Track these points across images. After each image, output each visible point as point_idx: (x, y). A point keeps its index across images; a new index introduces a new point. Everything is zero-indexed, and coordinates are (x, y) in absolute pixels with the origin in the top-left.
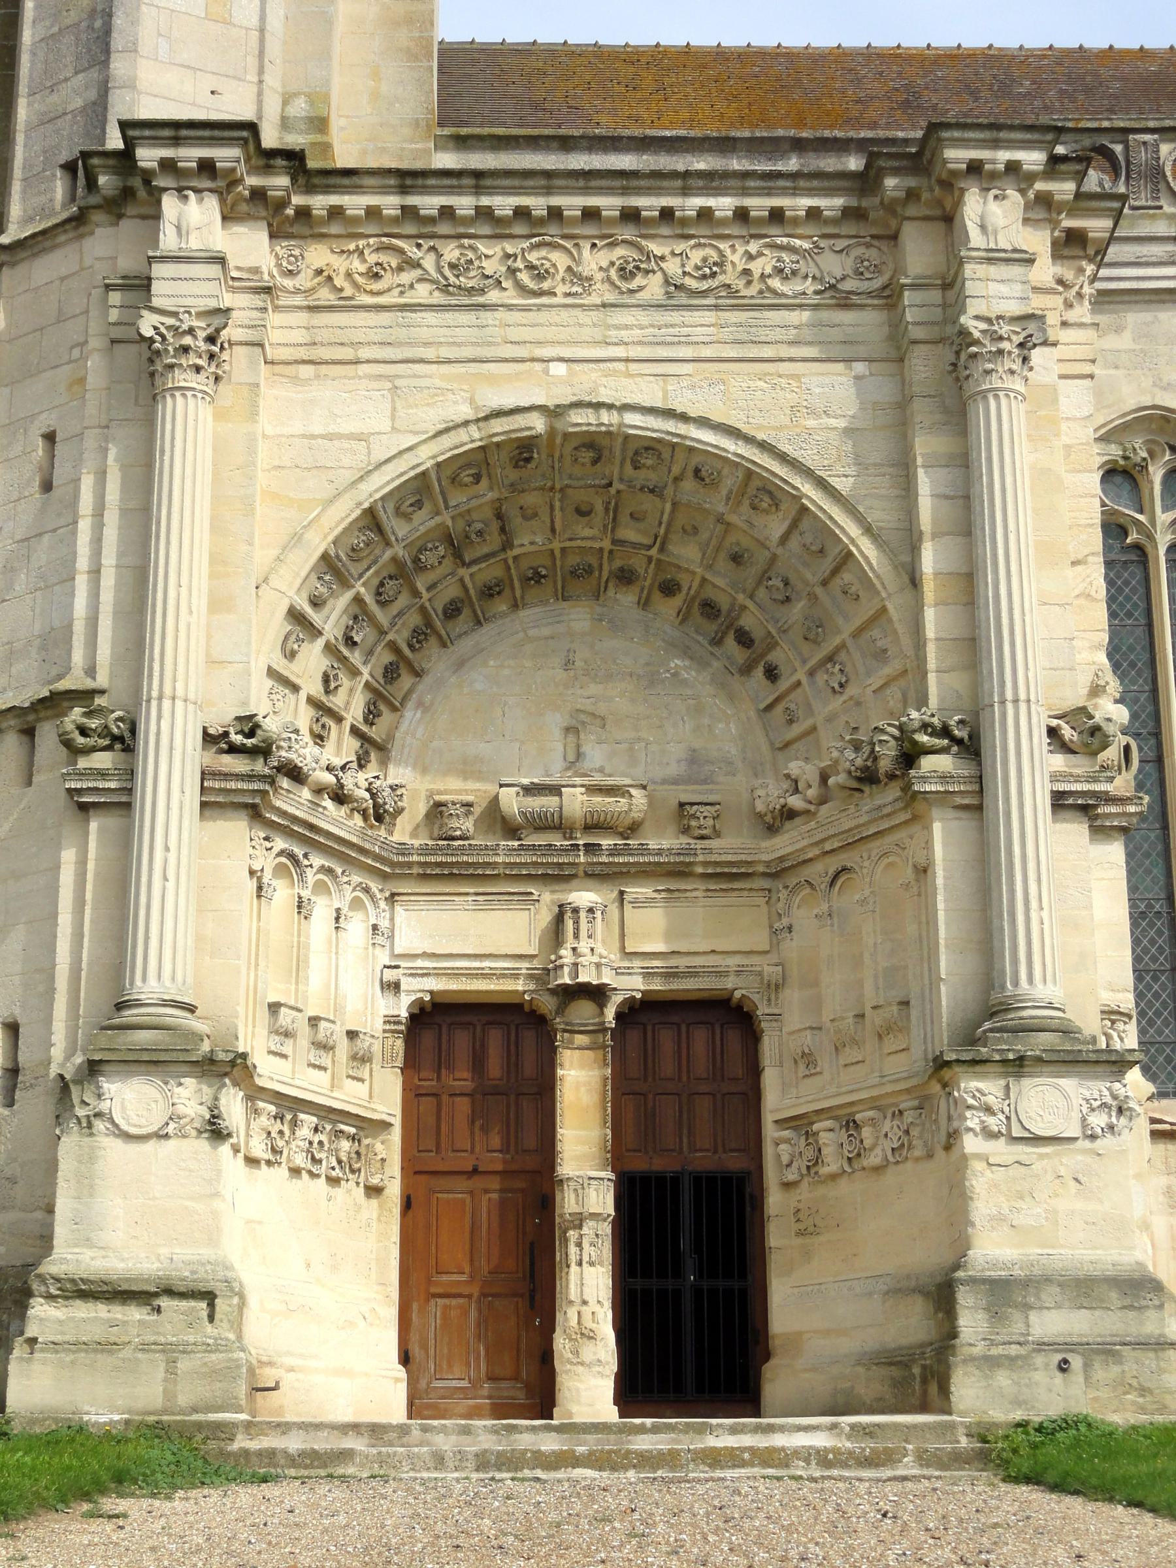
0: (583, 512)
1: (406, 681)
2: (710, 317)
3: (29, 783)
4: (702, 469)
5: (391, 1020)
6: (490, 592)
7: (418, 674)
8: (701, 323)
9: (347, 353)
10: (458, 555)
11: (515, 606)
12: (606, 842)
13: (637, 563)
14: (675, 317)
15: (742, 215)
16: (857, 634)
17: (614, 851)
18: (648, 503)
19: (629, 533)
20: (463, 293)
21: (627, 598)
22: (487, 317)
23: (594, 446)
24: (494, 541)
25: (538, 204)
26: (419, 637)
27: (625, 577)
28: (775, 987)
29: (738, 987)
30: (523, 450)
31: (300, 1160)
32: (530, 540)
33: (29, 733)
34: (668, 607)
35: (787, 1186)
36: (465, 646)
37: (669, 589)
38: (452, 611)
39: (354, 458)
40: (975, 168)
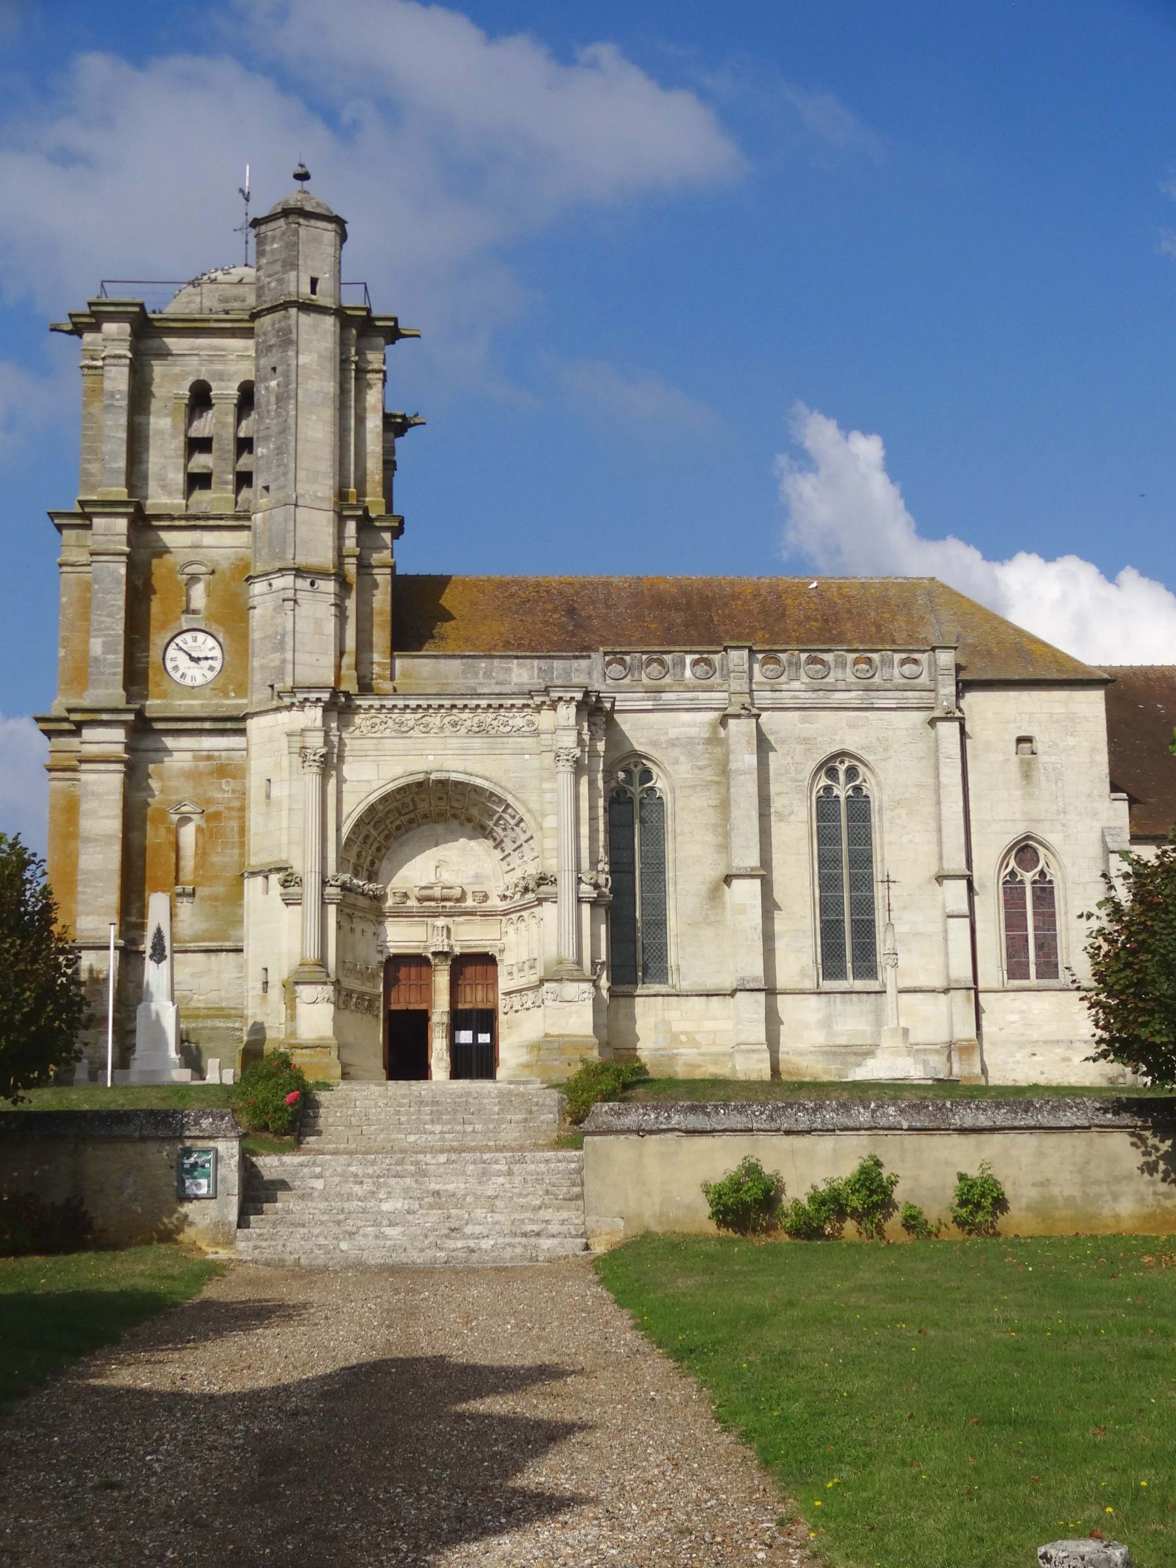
0: (440, 799)
1: (384, 850)
2: (479, 740)
3: (267, 893)
4: (477, 790)
5: (380, 962)
6: (411, 821)
7: (388, 849)
8: (477, 742)
9: (363, 753)
10: (399, 813)
11: (419, 825)
12: (448, 904)
13: (458, 812)
14: (469, 740)
15: (490, 706)
16: (526, 841)
17: (451, 907)
18: (460, 797)
19: (455, 804)
20: (402, 732)
21: (456, 822)
22: (407, 741)
23: (442, 783)
24: (412, 807)
25: (424, 703)
26: (387, 837)
27: (455, 816)
28: (502, 951)
29: (491, 951)
30: (420, 784)
31: (353, 1008)
32: (423, 807)
33: (266, 877)
34: (469, 826)
35: (506, 1013)
36: (403, 839)
37: (469, 820)
38: (398, 828)
39: (366, 788)
40: (560, 699)
